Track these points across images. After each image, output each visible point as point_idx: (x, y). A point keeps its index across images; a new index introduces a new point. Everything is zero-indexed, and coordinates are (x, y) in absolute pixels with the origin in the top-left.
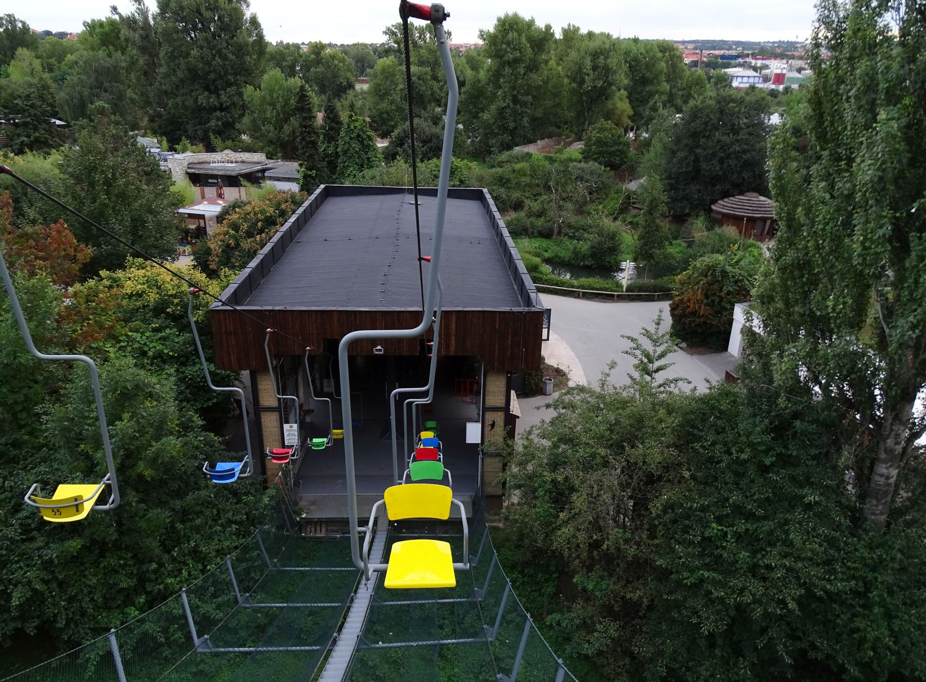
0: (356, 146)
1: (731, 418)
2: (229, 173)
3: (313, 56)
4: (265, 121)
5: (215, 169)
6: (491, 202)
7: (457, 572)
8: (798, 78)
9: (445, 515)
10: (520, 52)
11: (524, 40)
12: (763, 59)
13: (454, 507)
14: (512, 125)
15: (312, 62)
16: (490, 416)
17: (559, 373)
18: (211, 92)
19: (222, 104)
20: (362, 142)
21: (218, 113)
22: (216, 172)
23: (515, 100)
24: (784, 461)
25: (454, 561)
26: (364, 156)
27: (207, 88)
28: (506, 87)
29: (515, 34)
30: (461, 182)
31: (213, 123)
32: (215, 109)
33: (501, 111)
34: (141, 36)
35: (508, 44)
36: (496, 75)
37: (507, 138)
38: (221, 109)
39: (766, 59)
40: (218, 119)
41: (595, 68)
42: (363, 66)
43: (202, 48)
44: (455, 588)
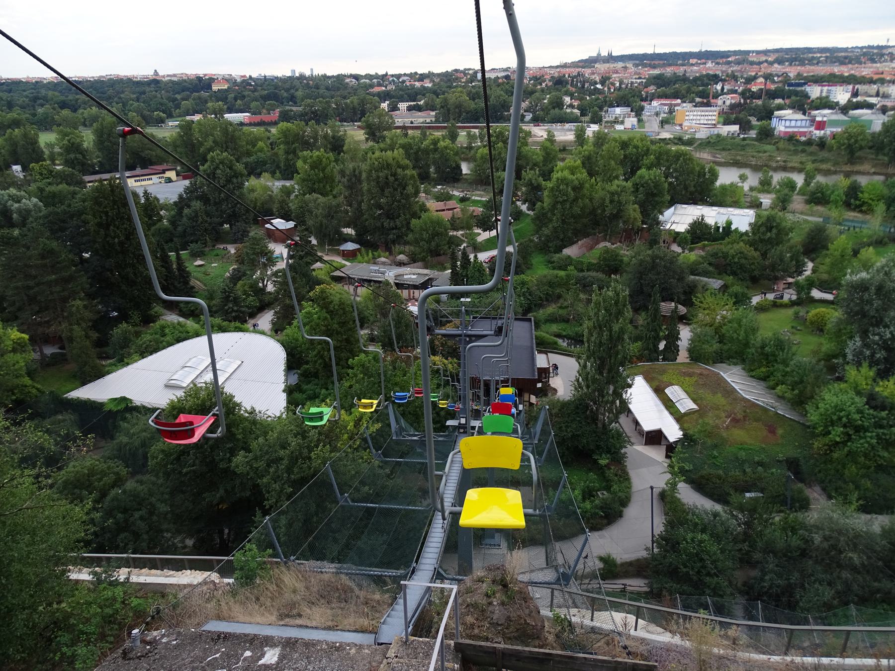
0: (477, 274)
1: (569, 404)
2: (414, 283)
3: (432, 147)
4: (422, 240)
5: (407, 280)
6: (533, 324)
7: (526, 515)
8: (843, 121)
9: (515, 465)
10: (567, 196)
11: (570, 189)
12: (829, 86)
13: (524, 459)
14: (562, 236)
15: (431, 150)
16: (525, 403)
17: (555, 390)
18: (391, 219)
19: (396, 226)
20: (480, 272)
21: (394, 231)
22: (408, 283)
23: (563, 222)
24: (577, 413)
25: (524, 507)
26: (481, 279)
27: (388, 217)
28: (559, 216)
29: (565, 187)
30: (528, 288)
31: (391, 236)
32: (393, 229)
33: (555, 228)
34: (348, 180)
35: (560, 191)
36: (554, 207)
37: (560, 243)
38: (396, 228)
39: (831, 86)
40: (394, 234)
41: (611, 201)
42: (460, 111)
43: (387, 197)
44: (524, 530)
